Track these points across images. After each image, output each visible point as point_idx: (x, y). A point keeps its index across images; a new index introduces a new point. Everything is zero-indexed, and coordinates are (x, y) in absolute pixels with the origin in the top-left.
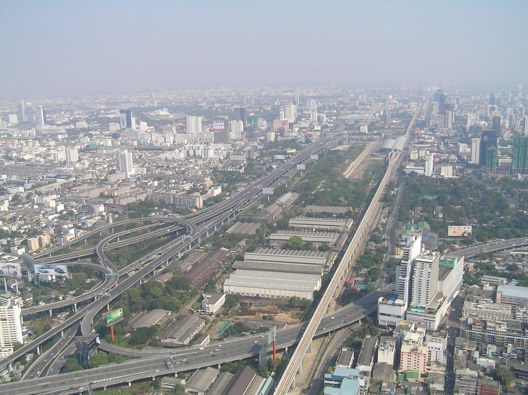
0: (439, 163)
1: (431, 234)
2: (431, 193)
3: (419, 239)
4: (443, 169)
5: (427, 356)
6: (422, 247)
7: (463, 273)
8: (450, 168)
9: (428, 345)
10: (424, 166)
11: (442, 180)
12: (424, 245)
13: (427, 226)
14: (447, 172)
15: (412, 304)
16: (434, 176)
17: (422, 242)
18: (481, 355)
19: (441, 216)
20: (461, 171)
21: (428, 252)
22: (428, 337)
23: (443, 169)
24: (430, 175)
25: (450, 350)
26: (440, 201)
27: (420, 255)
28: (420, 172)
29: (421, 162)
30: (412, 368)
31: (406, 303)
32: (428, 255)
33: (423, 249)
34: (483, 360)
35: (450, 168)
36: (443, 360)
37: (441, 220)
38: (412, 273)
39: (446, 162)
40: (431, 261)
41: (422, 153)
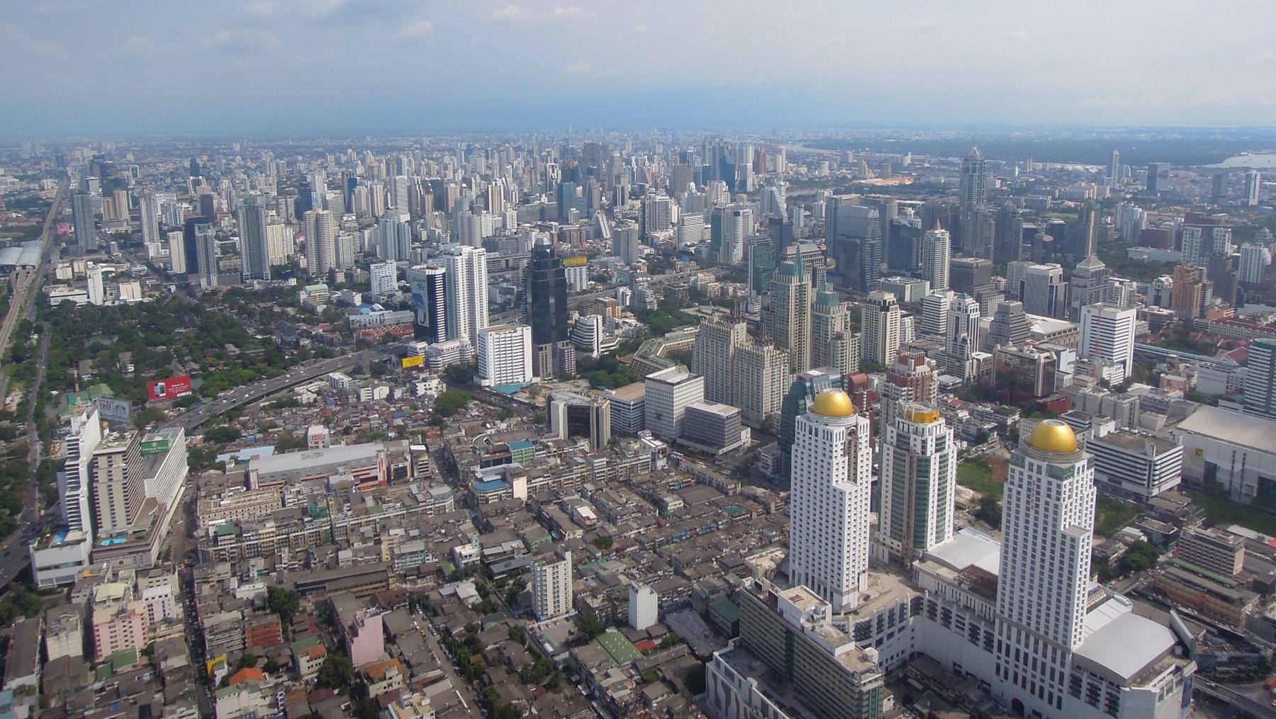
0: (111, 281)
1: (117, 403)
2: (108, 333)
3: (95, 417)
4: (123, 287)
5: (146, 616)
6: (102, 429)
7: (187, 455)
8: (136, 286)
9: (145, 596)
10: (86, 287)
11: (125, 308)
12: (106, 424)
13: (105, 389)
14: (131, 293)
15: (102, 533)
16: (109, 303)
17: (102, 420)
18: (242, 581)
19: (131, 368)
20: (155, 287)
21: (116, 434)
22: (142, 582)
23: (123, 287)
24: (99, 303)
25: (188, 590)
26: (127, 340)
27: (100, 444)
28: (81, 300)
29: (80, 281)
30: (121, 648)
31: (89, 537)
32: (116, 439)
33: (107, 431)
34: (246, 587)
35: (136, 286)
36: (176, 611)
37: (131, 376)
38: (92, 478)
39: (127, 276)
40: (124, 449)
41: (79, 266)
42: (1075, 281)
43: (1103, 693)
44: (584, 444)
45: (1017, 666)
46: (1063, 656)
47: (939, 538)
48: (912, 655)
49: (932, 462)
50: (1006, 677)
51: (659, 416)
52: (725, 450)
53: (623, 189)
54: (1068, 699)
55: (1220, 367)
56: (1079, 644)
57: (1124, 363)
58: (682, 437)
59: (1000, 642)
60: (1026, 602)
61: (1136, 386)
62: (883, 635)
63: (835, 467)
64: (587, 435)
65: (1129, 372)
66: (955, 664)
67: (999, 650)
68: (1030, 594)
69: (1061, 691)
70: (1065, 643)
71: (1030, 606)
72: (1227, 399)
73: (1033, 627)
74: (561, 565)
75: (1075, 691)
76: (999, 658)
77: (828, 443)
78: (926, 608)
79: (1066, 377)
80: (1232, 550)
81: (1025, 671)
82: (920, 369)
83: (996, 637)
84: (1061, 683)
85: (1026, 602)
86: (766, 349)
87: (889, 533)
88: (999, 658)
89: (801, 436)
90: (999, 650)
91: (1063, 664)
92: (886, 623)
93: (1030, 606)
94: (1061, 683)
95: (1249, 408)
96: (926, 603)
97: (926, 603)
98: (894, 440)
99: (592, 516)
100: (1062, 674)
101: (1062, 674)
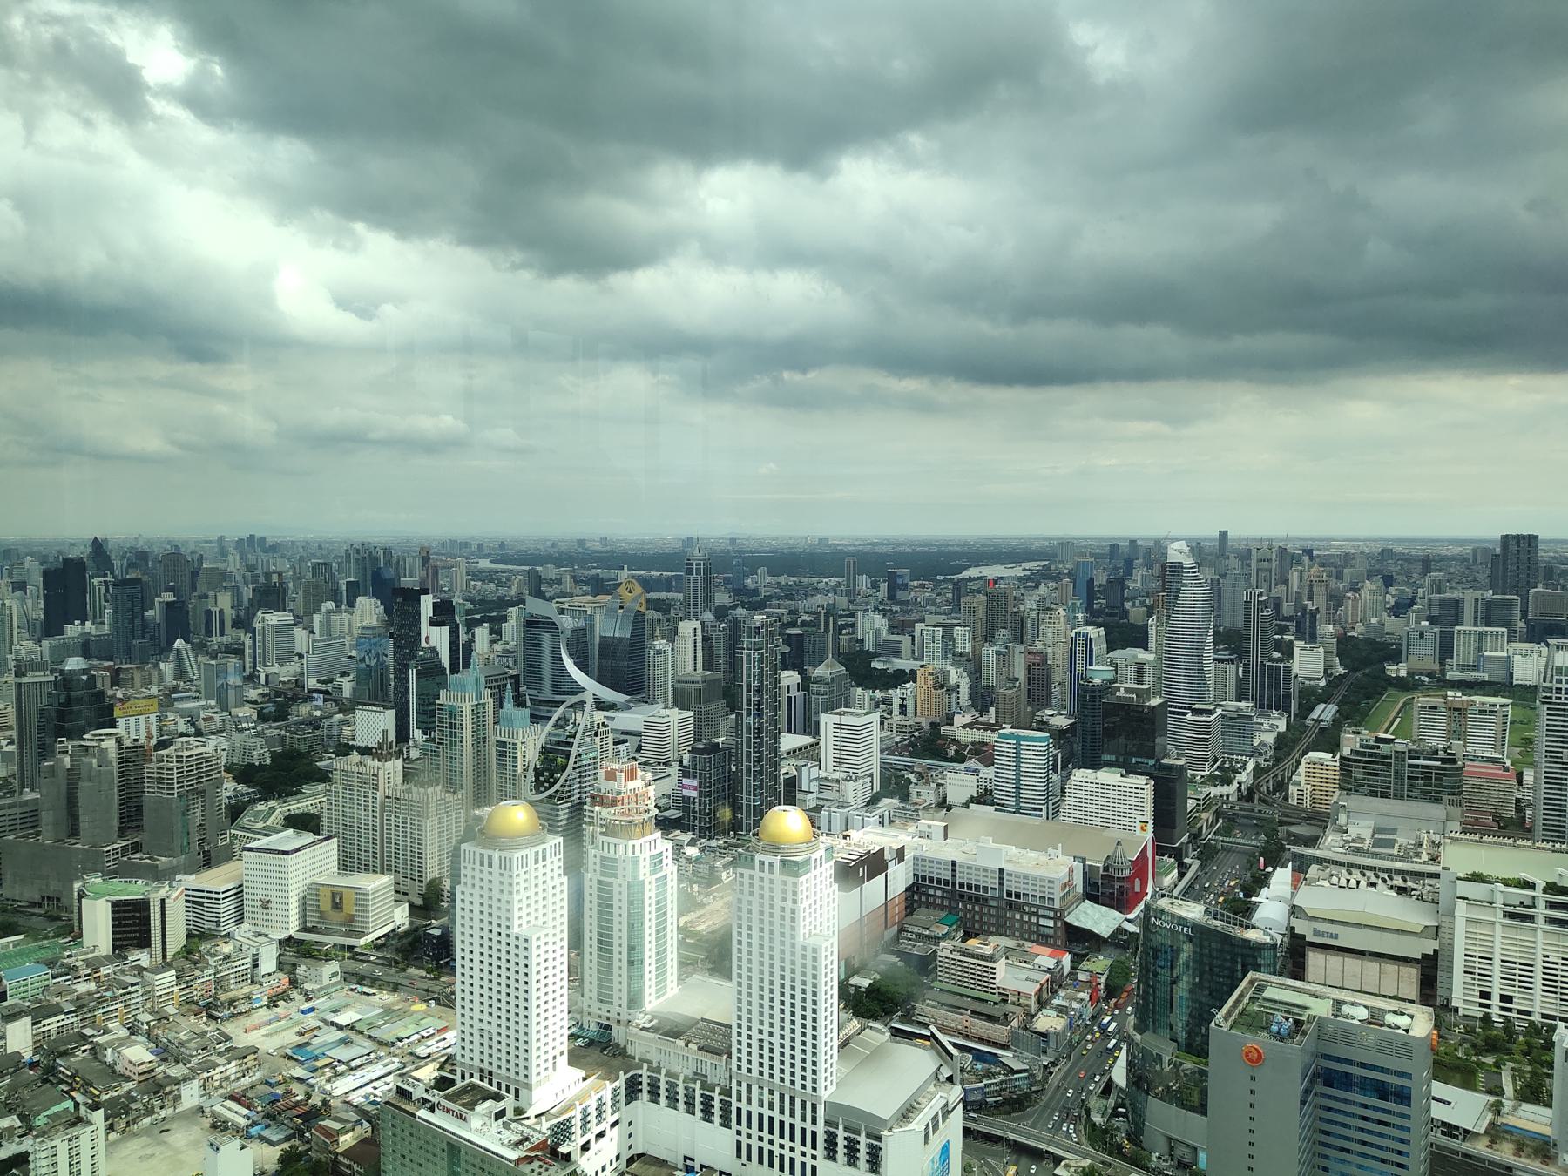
42: (814, 687)
43: (863, 1148)
44: (141, 957)
45: (761, 1139)
46: (814, 1107)
47: (660, 991)
48: (630, 1161)
49: (647, 887)
50: (749, 1158)
51: (265, 905)
52: (370, 938)
53: (221, 611)
54: (823, 1165)
55: (968, 771)
56: (831, 1089)
57: (871, 775)
58: (304, 929)
59: (739, 1110)
60: (766, 1046)
61: (885, 801)
62: (590, 1136)
63: (516, 906)
64: (144, 943)
65: (877, 788)
66: (686, 1158)
67: (739, 1123)
68: (771, 1034)
69: (814, 1157)
70: (814, 1090)
71: (772, 1051)
72: (979, 803)
73: (777, 1080)
74: (84, 1133)
75: (831, 1154)
76: (739, 1133)
77: (506, 874)
78: (645, 1088)
79: (810, 796)
80: (991, 959)
81: (771, 1142)
82: (632, 785)
83: (735, 1105)
84: (814, 1147)
85: (766, 1046)
86: (430, 790)
87: (595, 995)
88: (739, 1133)
89: (469, 872)
90: (739, 1123)
91: (814, 1121)
92: (593, 1118)
93: (772, 1051)
94: (814, 1147)
95: (1000, 807)
96: (645, 1081)
97: (645, 1081)
98: (598, 867)
99: (153, 1057)
100: (814, 1134)
101: (814, 1134)
